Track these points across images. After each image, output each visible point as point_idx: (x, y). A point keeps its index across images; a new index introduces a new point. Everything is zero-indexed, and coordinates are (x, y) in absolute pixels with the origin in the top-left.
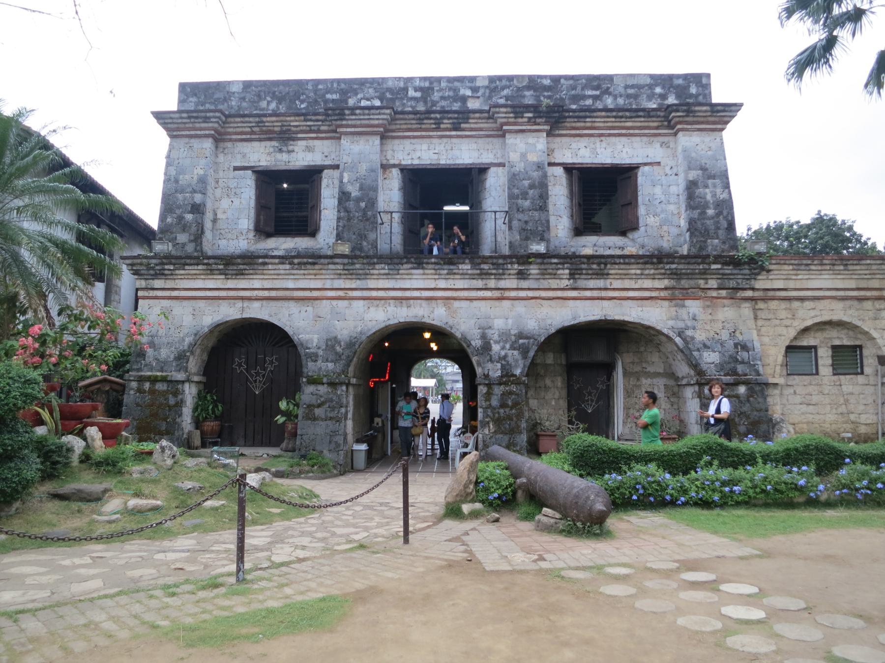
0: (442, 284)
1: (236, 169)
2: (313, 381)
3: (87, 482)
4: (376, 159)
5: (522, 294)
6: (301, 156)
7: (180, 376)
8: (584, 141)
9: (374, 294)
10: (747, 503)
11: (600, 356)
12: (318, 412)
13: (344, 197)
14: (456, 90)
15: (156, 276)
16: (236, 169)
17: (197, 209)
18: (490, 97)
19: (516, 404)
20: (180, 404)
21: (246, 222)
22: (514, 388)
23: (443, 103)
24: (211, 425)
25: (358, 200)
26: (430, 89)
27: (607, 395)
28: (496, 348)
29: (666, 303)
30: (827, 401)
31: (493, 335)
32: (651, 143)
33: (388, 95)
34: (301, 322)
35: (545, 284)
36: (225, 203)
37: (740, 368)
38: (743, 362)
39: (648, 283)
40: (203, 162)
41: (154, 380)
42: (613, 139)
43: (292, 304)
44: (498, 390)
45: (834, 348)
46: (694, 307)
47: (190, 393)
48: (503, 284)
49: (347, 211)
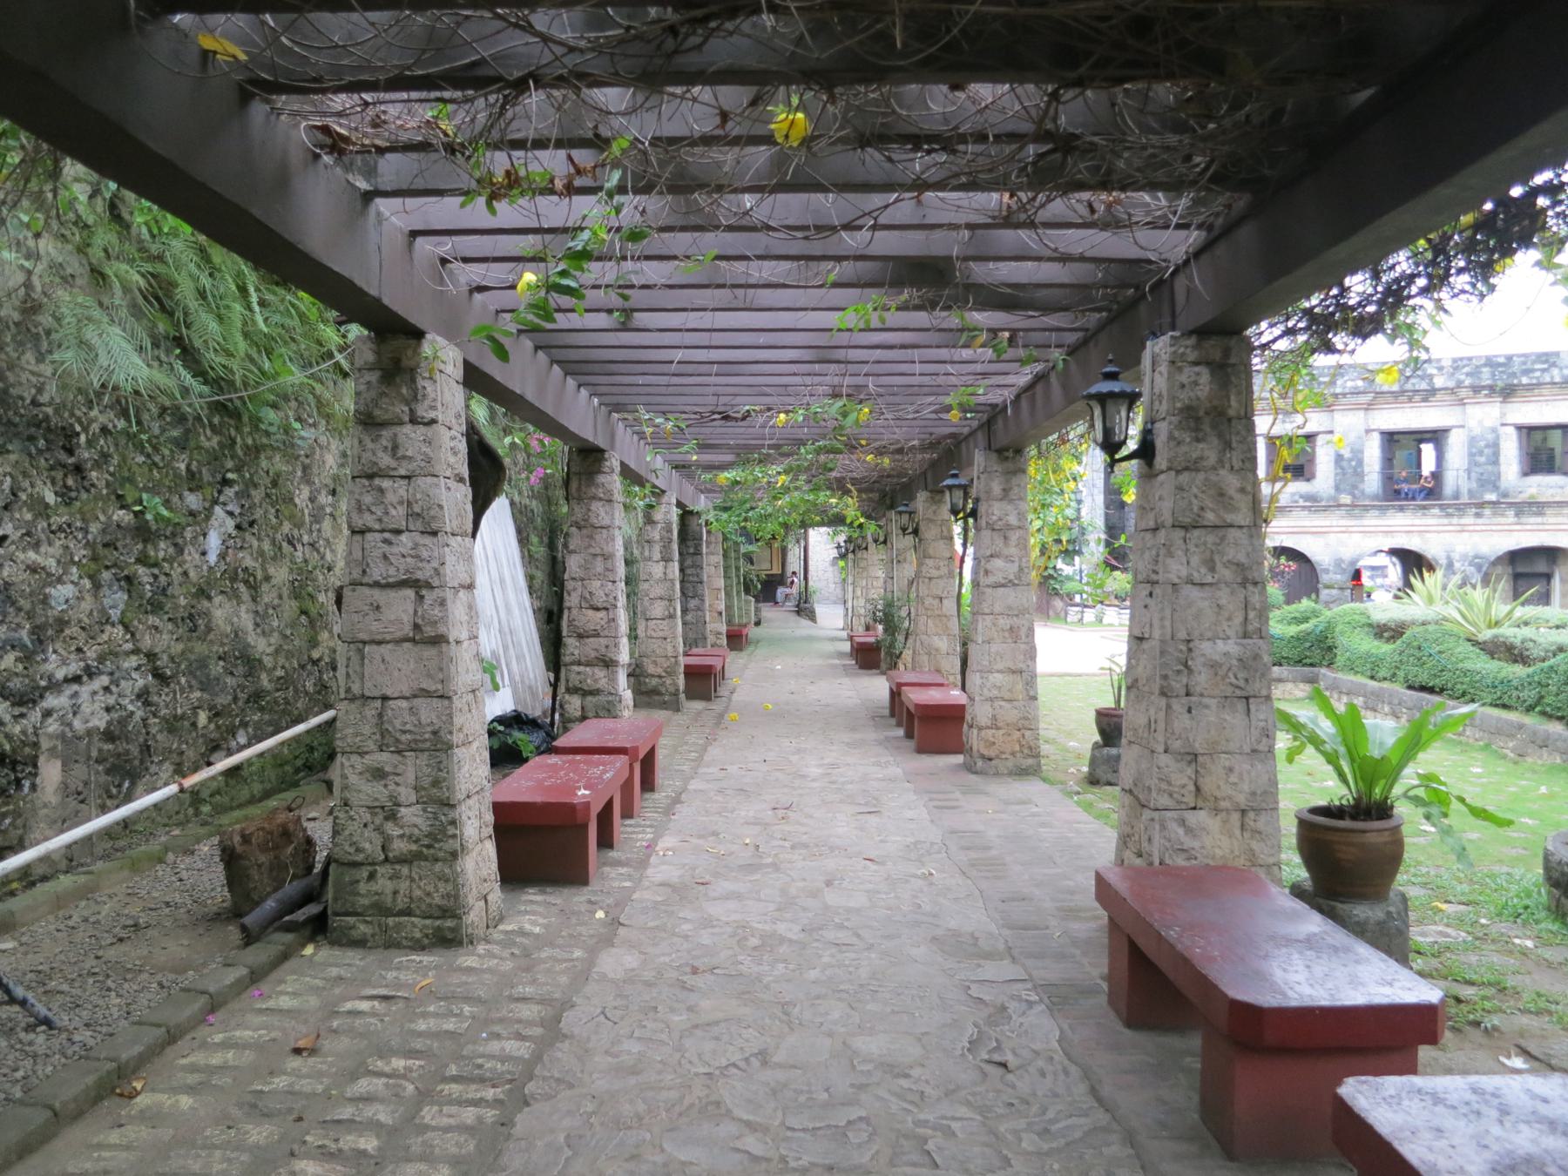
4: (1362, 428)
11: (1541, 567)
13: (1339, 458)
25: (1350, 460)
28: (1457, 565)
31: (1455, 556)
35: (1496, 520)
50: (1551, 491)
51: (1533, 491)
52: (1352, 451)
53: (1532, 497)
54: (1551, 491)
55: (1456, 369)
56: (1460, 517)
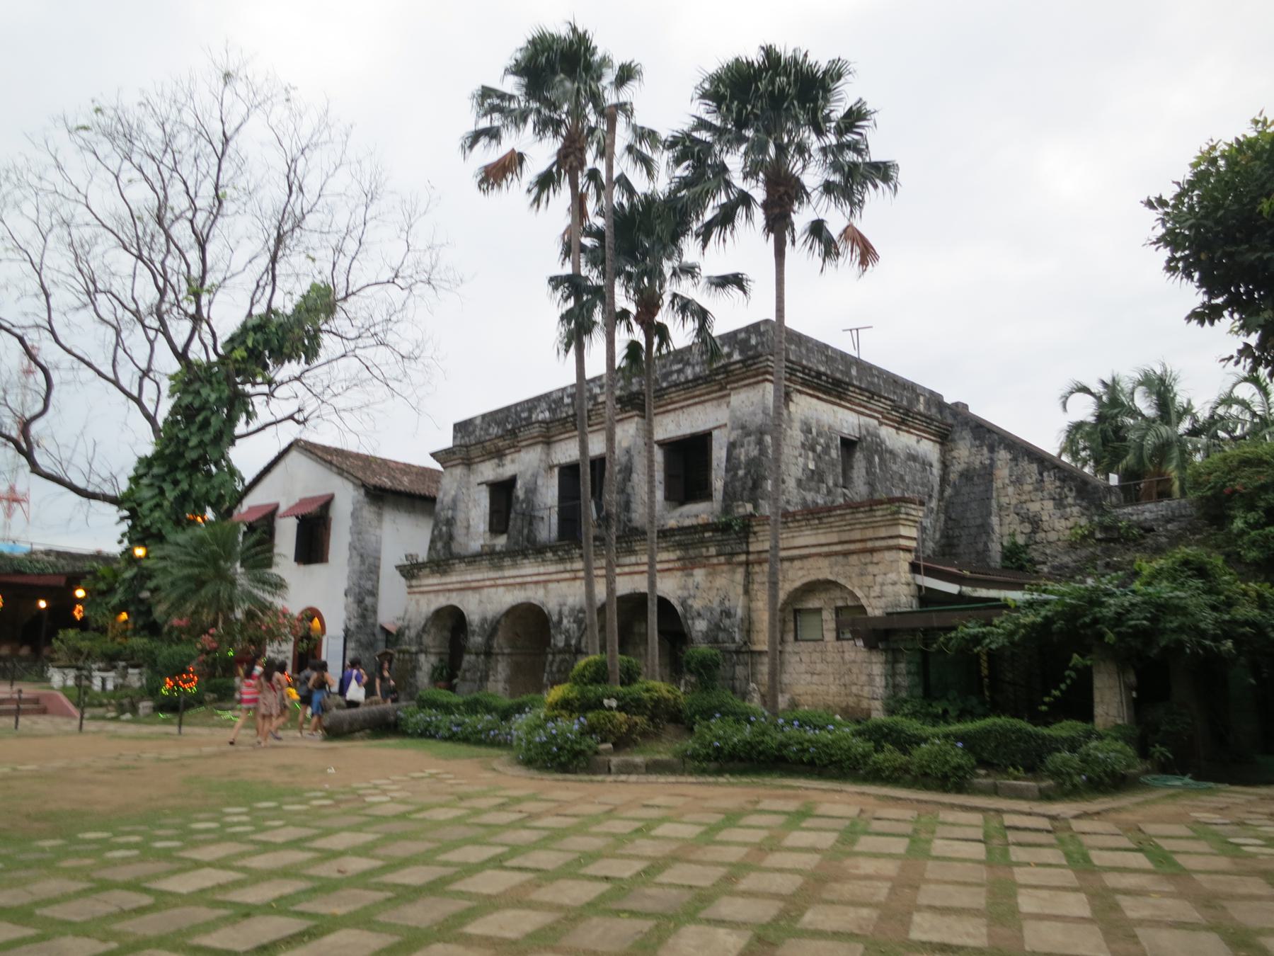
0: (542, 570)
6: (508, 470)
7: (414, 649)
8: (671, 416)
10: (466, 740)
22: (567, 656)
28: (565, 621)
29: (679, 574)
30: (830, 670)
31: (566, 610)
32: (719, 405)
37: (721, 636)
38: (725, 630)
42: (692, 409)
43: (470, 593)
44: (558, 658)
45: (838, 610)
46: (699, 574)
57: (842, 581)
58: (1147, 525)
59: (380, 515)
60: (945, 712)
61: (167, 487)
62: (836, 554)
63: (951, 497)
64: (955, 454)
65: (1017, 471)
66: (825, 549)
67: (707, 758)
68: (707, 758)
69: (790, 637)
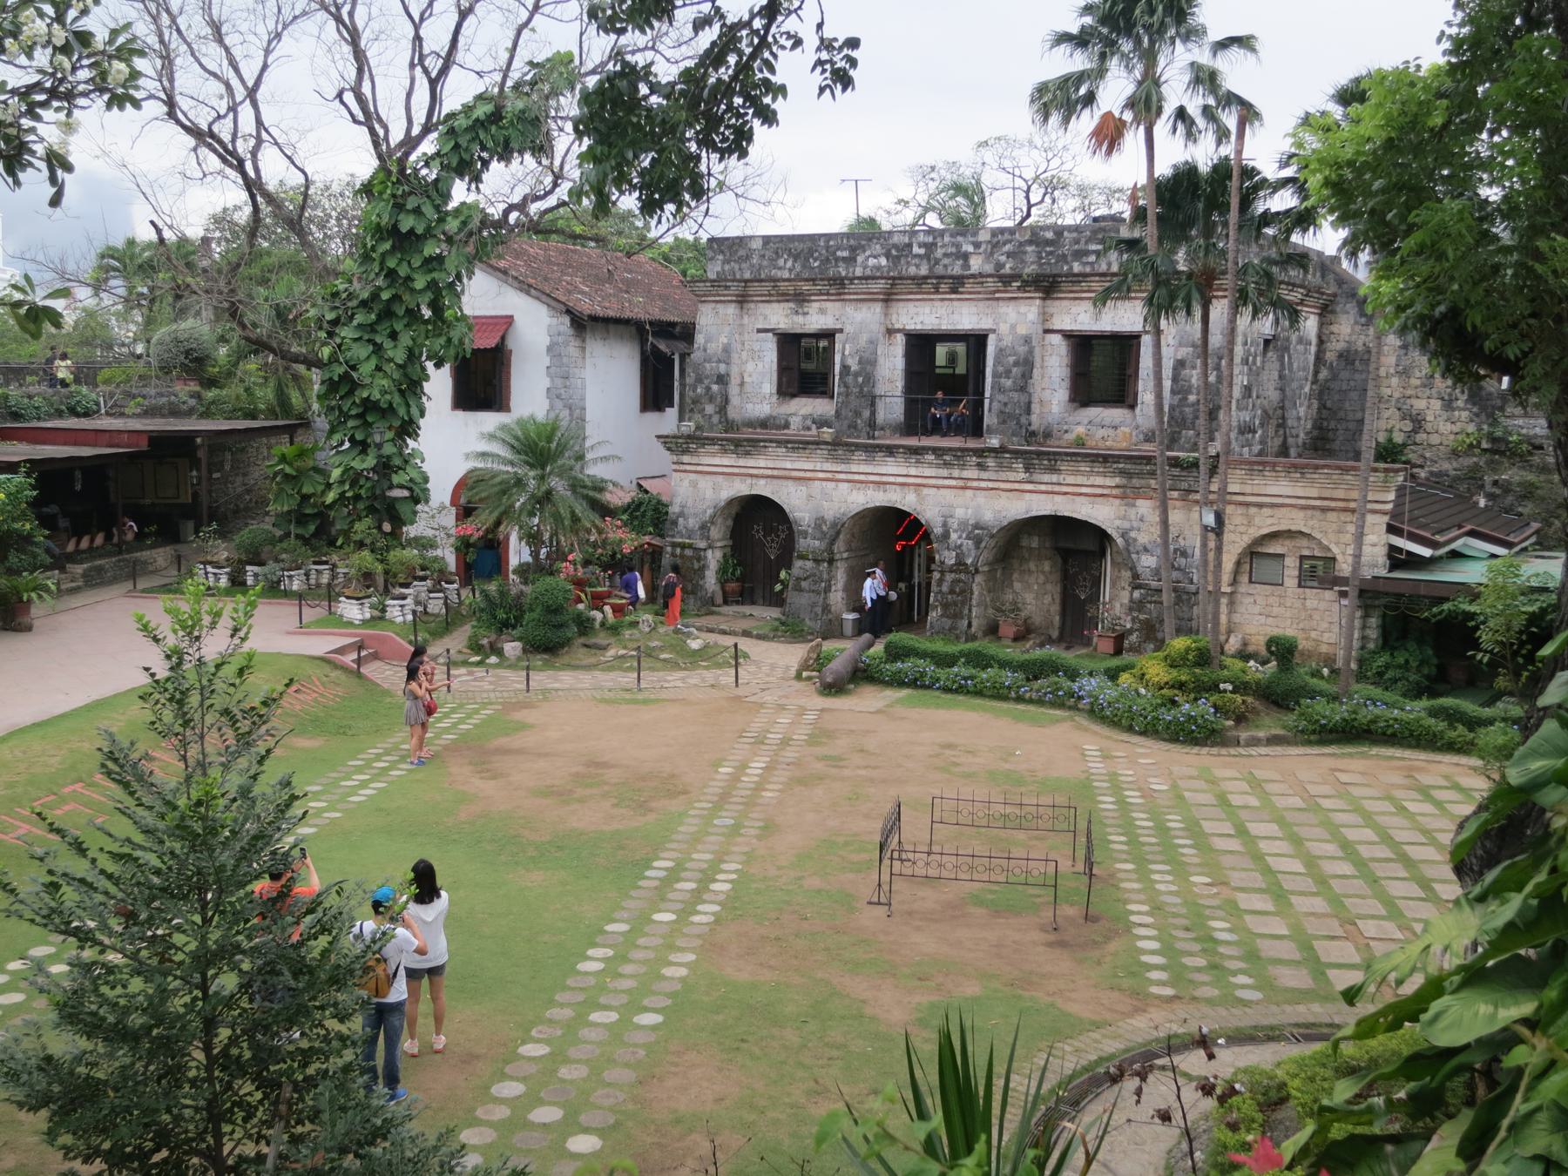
0: (913, 471)
1: (759, 331)
2: (802, 557)
3: (601, 638)
5: (983, 484)
6: (816, 318)
7: (702, 545)
9: (857, 477)
10: (979, 693)
12: (804, 584)
14: (958, 246)
15: (685, 451)
16: (759, 331)
17: (722, 379)
18: (992, 254)
19: (962, 592)
20: (703, 568)
21: (769, 386)
22: (963, 576)
23: (946, 261)
24: (733, 586)
25: (856, 375)
26: (934, 244)
27: (1097, 583)
28: (954, 536)
29: (1117, 502)
31: (954, 524)
33: (894, 252)
34: (798, 501)
35: (1003, 476)
36: (750, 367)
38: (1179, 569)
39: (1099, 480)
40: (727, 329)
41: (683, 546)
43: (790, 483)
44: (949, 577)
47: (713, 559)
48: (966, 474)
49: (846, 386)
50: (1101, 433)
51: (1081, 430)
52: (860, 362)
53: (1080, 442)
54: (1101, 433)
55: (995, 246)
56: (963, 467)
57: (1318, 536)
58: (1537, 442)
59: (583, 349)
60: (1407, 661)
61: (388, 344)
62: (1314, 508)
63: (1326, 381)
64: (1334, 328)
65: (1406, 362)
66: (1302, 502)
67: (1314, 732)
68: (1314, 732)
69: (1245, 578)
